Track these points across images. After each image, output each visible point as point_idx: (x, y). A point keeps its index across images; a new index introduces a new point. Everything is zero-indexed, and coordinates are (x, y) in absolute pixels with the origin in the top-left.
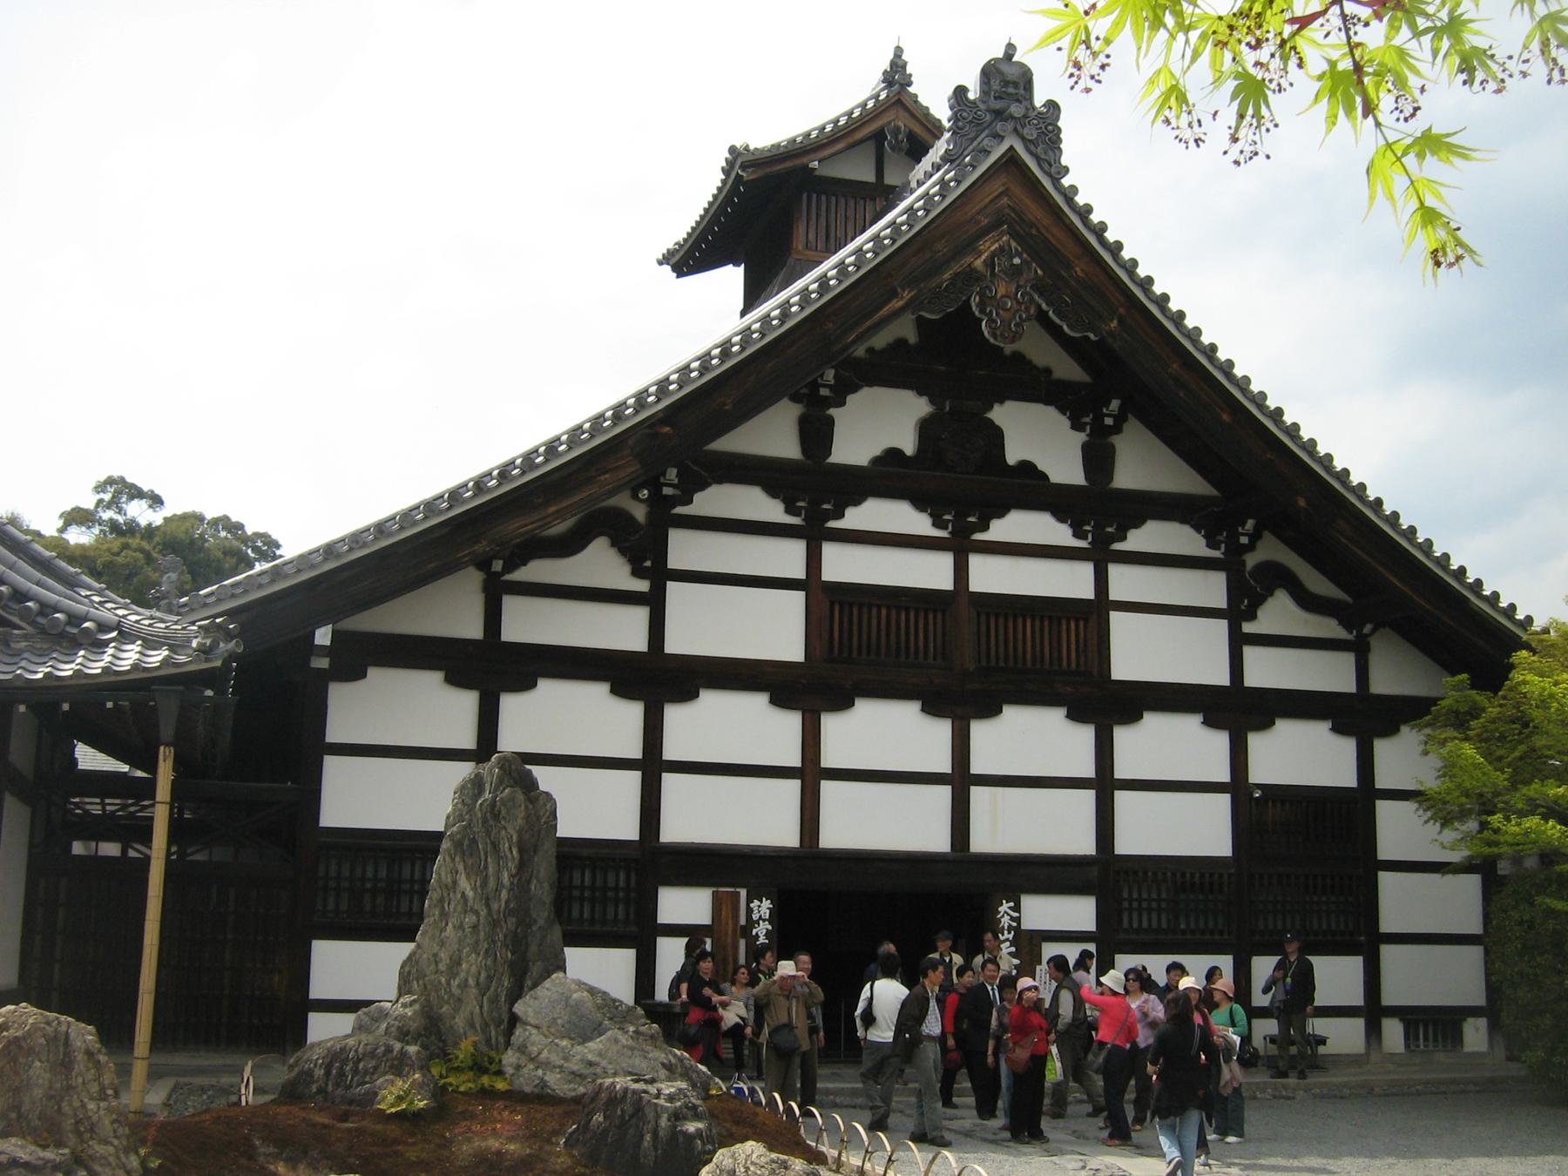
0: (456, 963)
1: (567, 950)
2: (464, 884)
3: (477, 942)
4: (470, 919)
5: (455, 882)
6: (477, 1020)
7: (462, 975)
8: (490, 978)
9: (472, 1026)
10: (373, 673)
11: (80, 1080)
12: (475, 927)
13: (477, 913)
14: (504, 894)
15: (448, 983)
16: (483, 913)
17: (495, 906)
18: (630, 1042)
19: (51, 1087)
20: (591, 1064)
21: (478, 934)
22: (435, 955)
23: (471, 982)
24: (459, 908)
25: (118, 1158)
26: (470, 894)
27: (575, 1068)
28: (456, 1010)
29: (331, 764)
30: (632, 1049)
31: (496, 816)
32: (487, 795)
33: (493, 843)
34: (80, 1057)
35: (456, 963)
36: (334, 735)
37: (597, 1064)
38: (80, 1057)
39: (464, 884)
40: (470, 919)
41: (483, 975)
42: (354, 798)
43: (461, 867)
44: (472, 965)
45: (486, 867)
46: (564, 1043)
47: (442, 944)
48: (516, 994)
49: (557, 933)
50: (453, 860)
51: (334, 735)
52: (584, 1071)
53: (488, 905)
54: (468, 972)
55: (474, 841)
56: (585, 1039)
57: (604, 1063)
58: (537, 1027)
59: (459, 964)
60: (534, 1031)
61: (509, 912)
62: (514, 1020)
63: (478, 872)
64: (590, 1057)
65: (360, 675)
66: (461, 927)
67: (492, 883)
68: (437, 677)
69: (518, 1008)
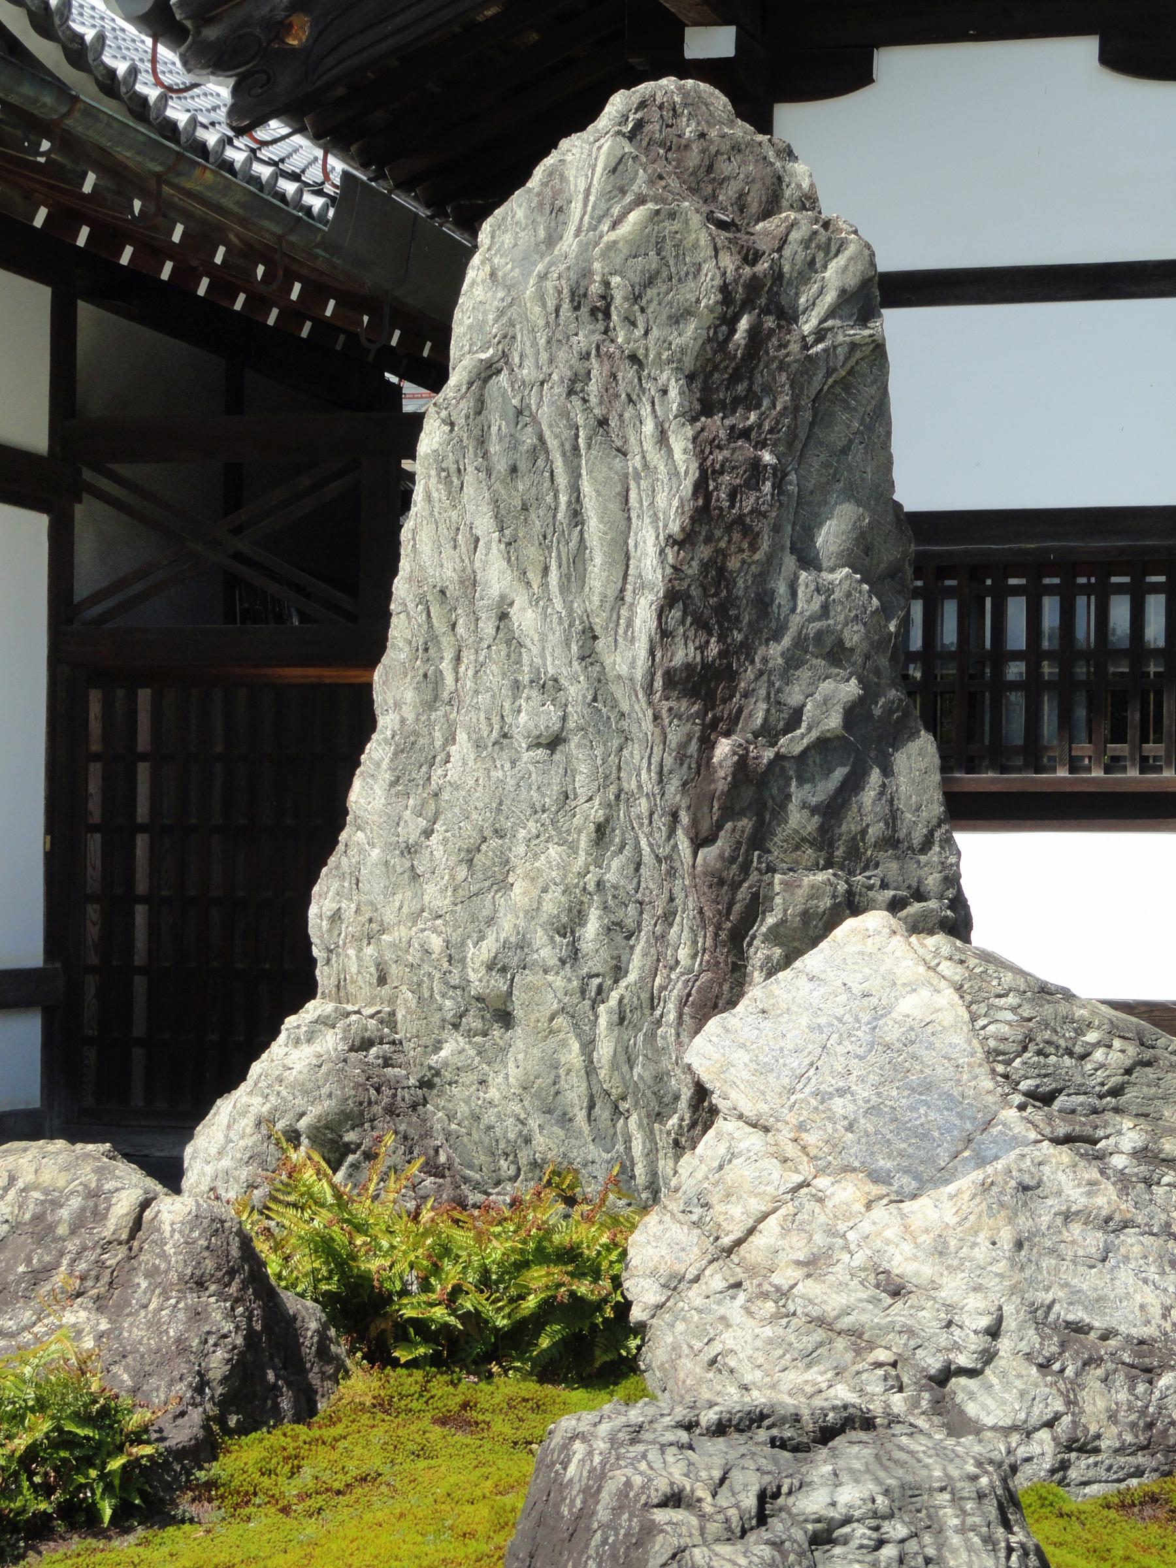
1: (965, 840)
5: (470, 583)
6: (575, 1093)
7: (507, 926)
8: (619, 932)
10: (895, 64)
12: (554, 743)
13: (550, 687)
14: (644, 614)
15: (454, 956)
16: (576, 691)
18: (1107, 1198)
26: (525, 618)
27: (833, 1303)
32: (569, 243)
35: (485, 866)
39: (496, 576)
40: (533, 715)
41: (592, 928)
43: (484, 525)
45: (577, 515)
46: (847, 1193)
48: (720, 992)
49: (917, 765)
50: (454, 491)
52: (868, 1317)
53: (588, 656)
54: (533, 913)
56: (927, 1178)
57: (952, 1288)
59: (504, 885)
60: (753, 1140)
62: (704, 1107)
64: (904, 1262)
68: (1080, 53)
69: (714, 1053)
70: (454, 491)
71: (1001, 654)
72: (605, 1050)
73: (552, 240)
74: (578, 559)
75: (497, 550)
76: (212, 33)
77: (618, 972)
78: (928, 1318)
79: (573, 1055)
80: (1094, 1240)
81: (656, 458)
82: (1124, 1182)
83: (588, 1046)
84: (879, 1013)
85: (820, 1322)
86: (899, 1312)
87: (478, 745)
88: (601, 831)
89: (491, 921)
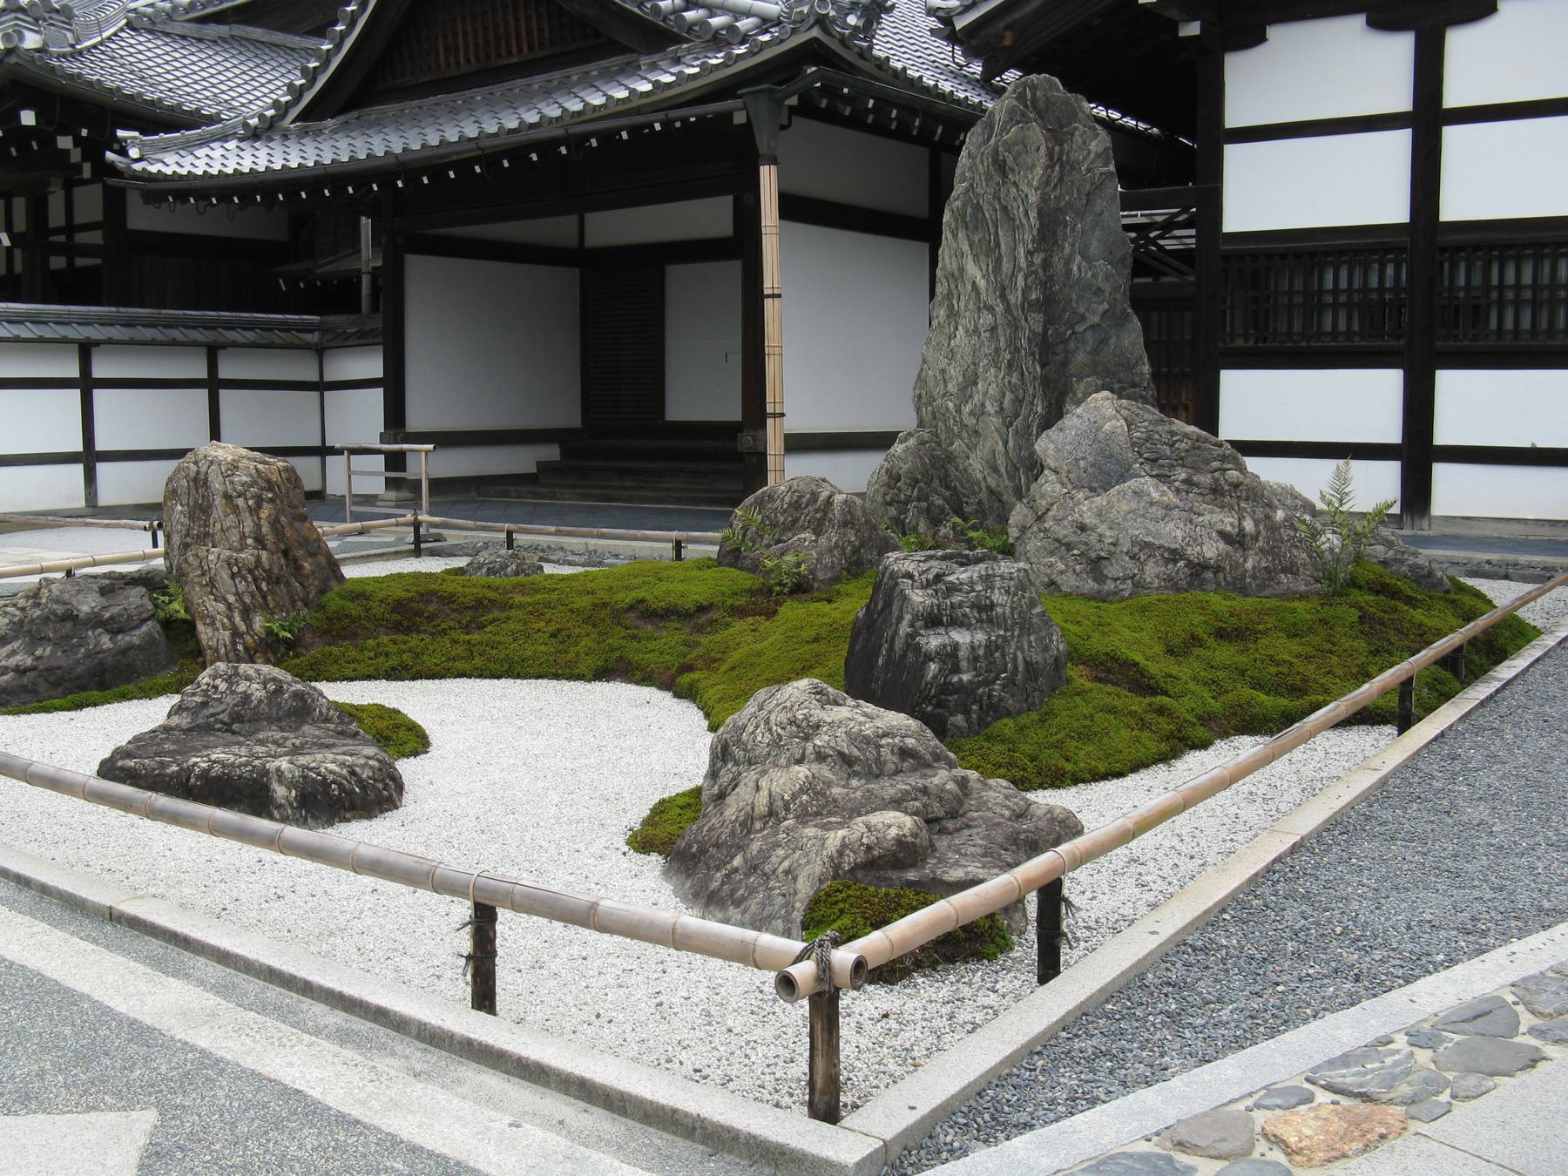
0: (971, 381)
2: (972, 269)
3: (997, 350)
4: (986, 319)
5: (962, 270)
8: (1018, 402)
9: (995, 469)
10: (1274, 32)
11: (218, 526)
12: (993, 330)
13: (991, 309)
15: (959, 411)
16: (1000, 309)
17: (1012, 299)
18: (1171, 497)
19: (187, 535)
20: (1083, 528)
21: (998, 340)
22: (943, 371)
23: (989, 408)
24: (971, 306)
25: (230, 618)
26: (982, 283)
28: (972, 447)
29: (1234, 155)
30: (1168, 508)
31: (1001, 167)
32: (993, 141)
33: (1005, 208)
34: (219, 501)
36: (1234, 118)
37: (1093, 529)
38: (219, 501)
39: (972, 269)
40: (986, 319)
42: (1262, 193)
43: (966, 248)
44: (991, 384)
45: (998, 245)
47: (952, 355)
50: (955, 237)
51: (1234, 118)
52: (1073, 538)
53: (1003, 297)
54: (985, 393)
55: (978, 207)
57: (1102, 528)
58: (1056, 472)
60: (1052, 477)
61: (1028, 306)
63: (989, 251)
64: (1088, 519)
65: (1259, 38)
66: (976, 331)
67: (1006, 266)
69: (1047, 445)
70: (955, 237)
71: (1321, 291)
72: (1011, 444)
73: (989, 139)
74: (998, 261)
75: (970, 259)
76: (974, 42)
77: (1017, 415)
78: (1093, 538)
79: (1000, 447)
80: (1161, 512)
81: (1024, 221)
82: (1178, 491)
83: (1006, 443)
84: (1099, 429)
85: (1057, 540)
86: (1083, 537)
87: (967, 332)
88: (1010, 365)
89: (971, 397)
